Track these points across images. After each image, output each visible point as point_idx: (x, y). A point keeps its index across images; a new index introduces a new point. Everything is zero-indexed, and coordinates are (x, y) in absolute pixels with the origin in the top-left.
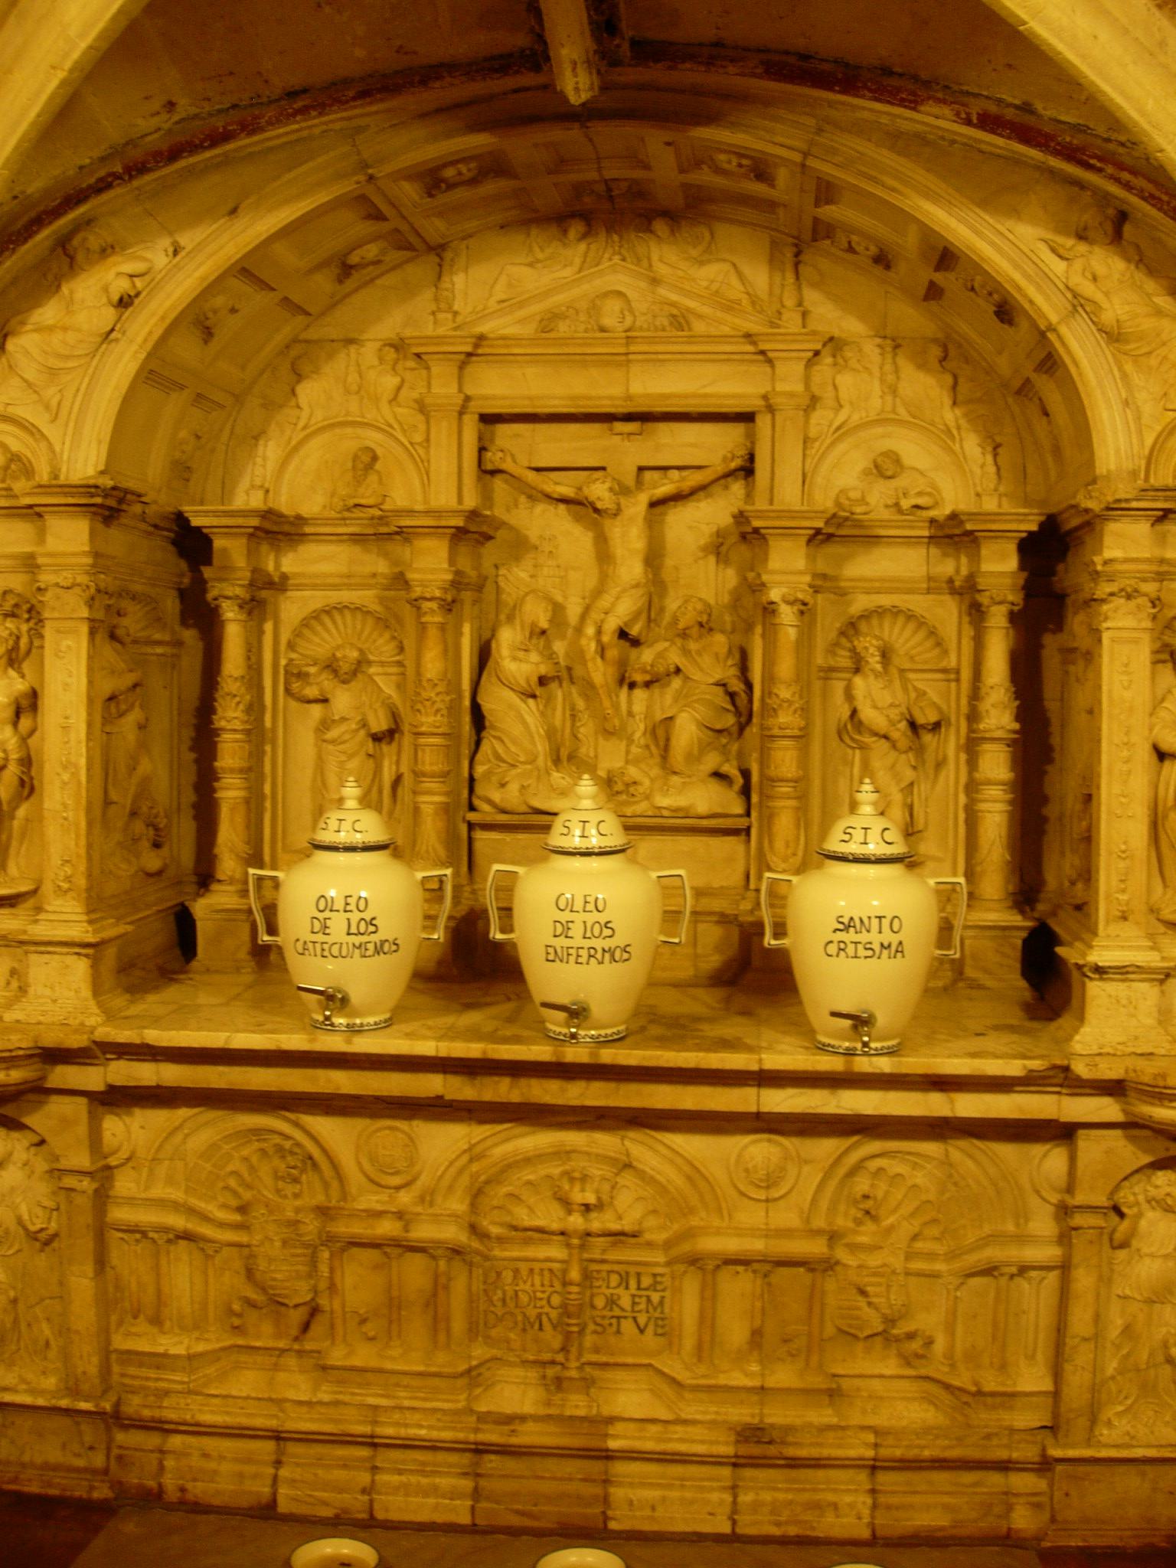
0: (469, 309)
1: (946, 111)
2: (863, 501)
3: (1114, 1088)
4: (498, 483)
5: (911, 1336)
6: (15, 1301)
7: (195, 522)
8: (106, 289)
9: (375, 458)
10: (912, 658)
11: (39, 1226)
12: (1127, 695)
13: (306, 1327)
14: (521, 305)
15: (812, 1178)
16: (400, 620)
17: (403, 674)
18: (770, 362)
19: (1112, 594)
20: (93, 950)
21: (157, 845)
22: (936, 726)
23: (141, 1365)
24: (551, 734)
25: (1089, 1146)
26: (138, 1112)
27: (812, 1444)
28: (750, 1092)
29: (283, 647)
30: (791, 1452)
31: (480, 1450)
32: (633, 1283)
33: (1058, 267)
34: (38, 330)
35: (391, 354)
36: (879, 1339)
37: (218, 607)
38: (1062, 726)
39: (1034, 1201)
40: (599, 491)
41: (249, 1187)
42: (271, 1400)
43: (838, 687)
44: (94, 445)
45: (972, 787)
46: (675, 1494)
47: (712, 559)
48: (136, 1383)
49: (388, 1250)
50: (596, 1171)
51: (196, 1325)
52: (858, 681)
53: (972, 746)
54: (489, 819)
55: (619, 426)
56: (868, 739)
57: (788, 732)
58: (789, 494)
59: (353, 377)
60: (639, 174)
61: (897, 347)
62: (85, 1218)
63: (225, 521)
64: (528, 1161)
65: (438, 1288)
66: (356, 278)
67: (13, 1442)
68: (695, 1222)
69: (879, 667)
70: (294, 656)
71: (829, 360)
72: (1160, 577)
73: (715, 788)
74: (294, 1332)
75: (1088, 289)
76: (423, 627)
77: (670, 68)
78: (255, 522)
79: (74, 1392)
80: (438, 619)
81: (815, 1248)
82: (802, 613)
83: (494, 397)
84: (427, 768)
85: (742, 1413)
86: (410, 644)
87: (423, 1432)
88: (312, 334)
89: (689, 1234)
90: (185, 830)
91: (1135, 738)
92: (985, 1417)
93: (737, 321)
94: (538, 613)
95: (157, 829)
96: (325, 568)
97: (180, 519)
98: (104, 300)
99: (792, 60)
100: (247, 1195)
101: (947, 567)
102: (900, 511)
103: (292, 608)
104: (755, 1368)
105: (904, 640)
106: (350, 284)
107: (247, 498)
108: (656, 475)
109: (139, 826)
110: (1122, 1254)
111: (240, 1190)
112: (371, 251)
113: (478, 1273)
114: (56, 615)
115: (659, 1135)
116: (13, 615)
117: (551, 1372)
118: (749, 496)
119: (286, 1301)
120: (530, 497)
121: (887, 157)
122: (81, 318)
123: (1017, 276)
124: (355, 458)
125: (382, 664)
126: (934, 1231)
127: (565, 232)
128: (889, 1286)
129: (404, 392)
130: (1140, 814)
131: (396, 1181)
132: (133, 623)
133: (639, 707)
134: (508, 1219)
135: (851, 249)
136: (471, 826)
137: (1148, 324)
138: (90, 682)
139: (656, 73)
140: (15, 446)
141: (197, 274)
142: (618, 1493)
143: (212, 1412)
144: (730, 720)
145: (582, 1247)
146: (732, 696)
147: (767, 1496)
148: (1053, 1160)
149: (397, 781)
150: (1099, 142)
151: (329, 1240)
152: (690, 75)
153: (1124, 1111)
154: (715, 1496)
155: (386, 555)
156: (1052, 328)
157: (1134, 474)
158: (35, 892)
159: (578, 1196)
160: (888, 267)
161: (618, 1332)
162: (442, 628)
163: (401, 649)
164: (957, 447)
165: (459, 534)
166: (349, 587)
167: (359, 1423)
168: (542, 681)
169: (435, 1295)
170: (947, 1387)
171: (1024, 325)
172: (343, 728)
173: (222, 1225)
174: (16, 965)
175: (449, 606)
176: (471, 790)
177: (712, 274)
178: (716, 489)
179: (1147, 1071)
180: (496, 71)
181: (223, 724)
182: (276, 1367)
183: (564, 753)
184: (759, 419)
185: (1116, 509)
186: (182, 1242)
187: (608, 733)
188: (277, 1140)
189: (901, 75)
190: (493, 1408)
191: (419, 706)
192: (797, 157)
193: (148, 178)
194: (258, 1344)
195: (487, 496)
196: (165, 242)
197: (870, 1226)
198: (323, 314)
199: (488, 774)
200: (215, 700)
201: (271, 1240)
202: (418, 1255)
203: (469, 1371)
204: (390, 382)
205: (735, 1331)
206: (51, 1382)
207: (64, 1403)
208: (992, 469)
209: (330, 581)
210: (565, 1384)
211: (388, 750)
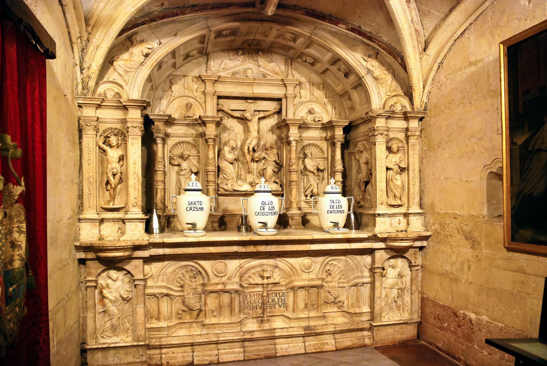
0: (215, 70)
1: (344, 27)
2: (307, 119)
6: (119, 318)
7: (151, 117)
9: (192, 105)
10: (316, 156)
11: (127, 296)
12: (381, 156)
13: (198, 315)
14: (228, 70)
15: (318, 266)
16: (198, 145)
17: (200, 159)
18: (286, 87)
23: (154, 331)
25: (378, 254)
28: (308, 245)
29: (168, 152)
32: (278, 295)
33: (364, 63)
35: (195, 80)
37: (156, 139)
38: (349, 171)
39: (364, 268)
40: (248, 115)
41: (183, 280)
42: (190, 335)
44: (137, 92)
47: (271, 133)
48: (153, 336)
49: (219, 293)
50: (269, 269)
51: (169, 318)
55: (249, 101)
56: (308, 173)
61: (313, 84)
64: (253, 267)
66: (189, 59)
68: (293, 279)
71: (298, 87)
72: (388, 131)
73: (276, 184)
74: (195, 317)
78: (167, 118)
79: (138, 341)
80: (212, 144)
81: (319, 283)
82: (297, 143)
84: (211, 180)
88: (175, 73)
89: (292, 282)
91: (383, 165)
93: (278, 77)
94: (232, 143)
100: (182, 283)
103: (171, 142)
104: (306, 313)
106: (186, 61)
111: (181, 282)
112: (194, 52)
113: (241, 296)
114: (132, 134)
117: (259, 319)
119: (194, 309)
120: (227, 117)
121: (329, 36)
123: (356, 65)
124: (187, 105)
125: (193, 156)
126: (344, 277)
127: (238, 53)
129: (199, 89)
131: (222, 275)
133: (255, 167)
134: (248, 282)
135: (306, 61)
137: (383, 76)
143: (175, 341)
144: (276, 170)
145: (266, 287)
146: (277, 163)
148: (368, 259)
153: (386, 245)
155: (195, 129)
156: (363, 77)
157: (380, 109)
158: (124, 207)
161: (275, 308)
163: (199, 152)
164: (327, 107)
166: (186, 137)
168: (235, 159)
171: (352, 78)
172: (185, 171)
173: (176, 291)
174: (120, 226)
175: (214, 140)
176: (218, 186)
177: (272, 65)
178: (271, 116)
179: (393, 235)
181: (158, 169)
182: (191, 327)
184: (283, 100)
185: (379, 116)
186: (165, 297)
189: (334, 17)
190: (247, 330)
191: (208, 165)
192: (309, 35)
194: (186, 321)
197: (330, 277)
198: (178, 68)
200: (155, 163)
201: (190, 293)
202: (227, 294)
203: (240, 322)
204: (195, 86)
205: (301, 305)
208: (334, 112)
209: (181, 135)
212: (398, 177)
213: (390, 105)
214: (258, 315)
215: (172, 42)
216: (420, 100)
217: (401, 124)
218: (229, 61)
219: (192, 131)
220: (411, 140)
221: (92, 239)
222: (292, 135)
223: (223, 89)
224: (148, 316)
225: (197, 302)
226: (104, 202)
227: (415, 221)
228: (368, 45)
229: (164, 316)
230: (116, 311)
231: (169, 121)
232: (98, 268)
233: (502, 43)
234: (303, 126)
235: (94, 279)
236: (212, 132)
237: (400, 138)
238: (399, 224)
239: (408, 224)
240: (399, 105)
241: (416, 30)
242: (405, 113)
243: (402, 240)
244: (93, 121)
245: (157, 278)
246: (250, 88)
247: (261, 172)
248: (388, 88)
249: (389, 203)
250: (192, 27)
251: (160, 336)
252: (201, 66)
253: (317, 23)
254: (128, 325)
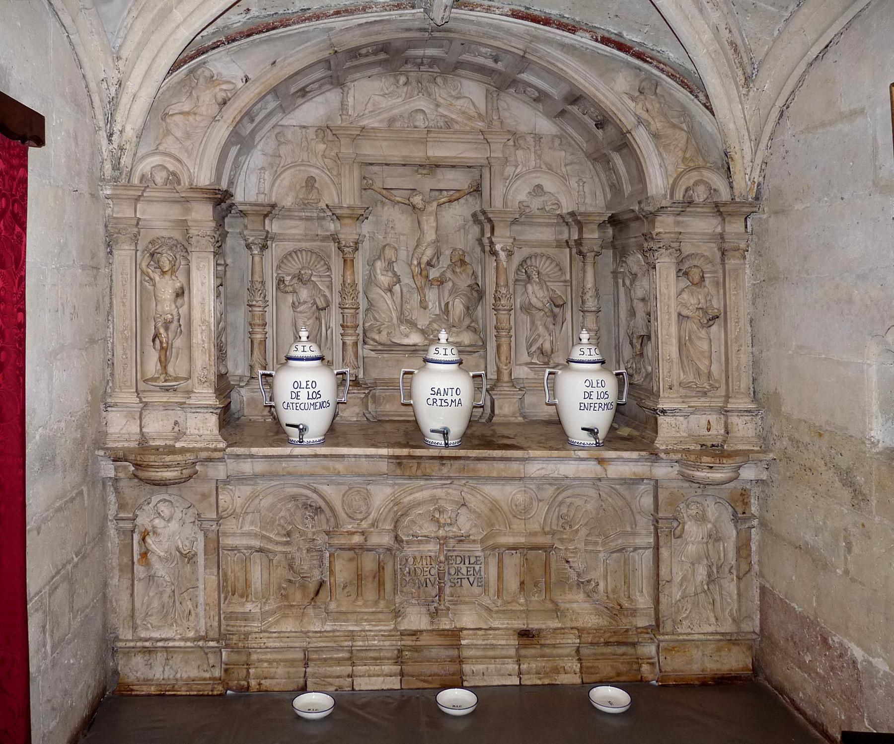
65: (381, 568)
98: (214, 101)
131: (360, 516)
229: (256, 589)
250: (303, 46)
254: (190, 606)
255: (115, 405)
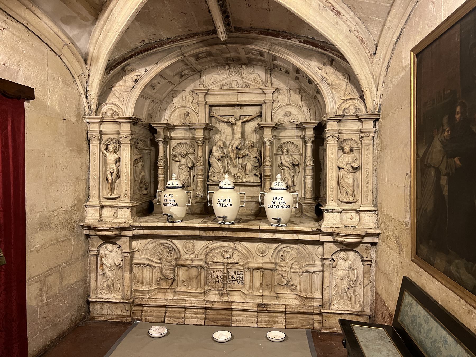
3: (331, 234)
4: (213, 119)
5: (292, 285)
6: (113, 280)
7: (153, 126)
8: (132, 78)
9: (189, 114)
12: (332, 156)
13: (172, 284)
14: (217, 83)
15: (272, 251)
19: (329, 136)
20: (131, 208)
21: (146, 189)
22: (298, 165)
24: (224, 167)
26: (140, 240)
27: (272, 308)
30: (268, 309)
31: (206, 309)
32: (237, 273)
34: (119, 86)
36: (286, 286)
37: (158, 142)
39: (316, 258)
40: (232, 120)
41: (162, 255)
42: (165, 299)
43: (279, 158)
45: (305, 177)
46: (245, 318)
47: (254, 133)
48: (137, 296)
52: (282, 157)
53: (304, 169)
54: (211, 183)
56: (284, 168)
57: (268, 166)
58: (269, 120)
59: (184, 97)
60: (238, 55)
62: (128, 262)
63: (159, 126)
67: (111, 310)
68: (249, 260)
69: (286, 153)
70: (174, 152)
71: (277, 93)
72: (339, 133)
73: (255, 177)
74: (170, 285)
75: (325, 75)
76: (198, 146)
77: (242, 33)
78: (165, 126)
79: (124, 299)
80: (201, 145)
81: (273, 266)
82: (271, 143)
83: (211, 102)
84: (200, 173)
85: (259, 301)
86: (196, 150)
87: (195, 305)
89: (247, 263)
90: (152, 186)
91: (334, 165)
92: (308, 303)
95: (146, 186)
96: (179, 135)
97: (150, 125)
99: (266, 30)
100: (161, 257)
101: (300, 134)
102: (291, 123)
103: (173, 143)
104: (261, 291)
105: (292, 148)
107: (164, 121)
108: (243, 117)
109: (142, 185)
110: (335, 269)
112: (186, 72)
113: (206, 271)
115: (241, 243)
116: (115, 143)
117: (220, 292)
118: (261, 121)
121: (285, 51)
122: (127, 84)
124: (185, 113)
125: (191, 154)
126: (296, 263)
128: (287, 275)
129: (194, 101)
130: (335, 180)
131: (190, 253)
132: (140, 145)
133: (240, 162)
136: (208, 185)
138: (131, 156)
139: (239, 34)
140: (115, 109)
141: (150, 76)
142: (234, 318)
145: (227, 266)
146: (258, 160)
147: (264, 319)
148: (320, 249)
149: (194, 177)
150: (328, 45)
151: (177, 265)
152: (246, 34)
154: (253, 319)
157: (334, 112)
158: (120, 197)
159: (226, 255)
160: (288, 74)
162: (202, 146)
165: (205, 129)
166: (184, 139)
167: (182, 303)
168: (222, 157)
169: (198, 276)
170: (300, 296)
173: (156, 263)
175: (203, 143)
178: (255, 119)
179: (337, 230)
180: (208, 34)
182: (166, 292)
183: (226, 171)
185: (329, 120)
187: (234, 167)
188: (167, 245)
190: (209, 300)
192: (267, 51)
193: (140, 56)
195: (211, 121)
196: (144, 69)
197: (283, 262)
198: (178, 85)
199: (211, 175)
202: (195, 268)
203: (205, 292)
204: (191, 99)
205: (257, 284)
206: (120, 297)
207: (122, 301)
210: (223, 294)
211: (192, 171)
212: (350, 175)
213: (343, 108)
214: (220, 289)
215: (155, 69)
216: (374, 102)
217: (356, 126)
218: (217, 76)
219: (189, 135)
220: (364, 141)
221: (93, 221)
222: (266, 136)
223: (212, 99)
224: (133, 279)
225: (171, 273)
226: (106, 192)
227: (366, 218)
228: (324, 54)
229: (147, 281)
230: (110, 275)
231: (170, 127)
232: (99, 242)
233: (412, 50)
234: (277, 127)
235: (96, 249)
236: (200, 136)
237: (354, 139)
238: (351, 219)
239: (360, 221)
240: (352, 107)
241: (359, 38)
242: (357, 116)
243: (345, 236)
244: (97, 133)
245: (142, 252)
246: (236, 97)
247: (244, 167)
248: (342, 93)
249: (341, 200)
251: (142, 296)
252: (195, 81)
253: (274, 39)
255: (89, 206)
